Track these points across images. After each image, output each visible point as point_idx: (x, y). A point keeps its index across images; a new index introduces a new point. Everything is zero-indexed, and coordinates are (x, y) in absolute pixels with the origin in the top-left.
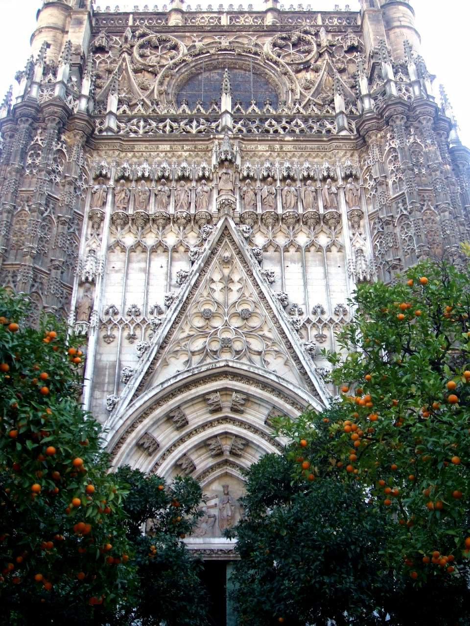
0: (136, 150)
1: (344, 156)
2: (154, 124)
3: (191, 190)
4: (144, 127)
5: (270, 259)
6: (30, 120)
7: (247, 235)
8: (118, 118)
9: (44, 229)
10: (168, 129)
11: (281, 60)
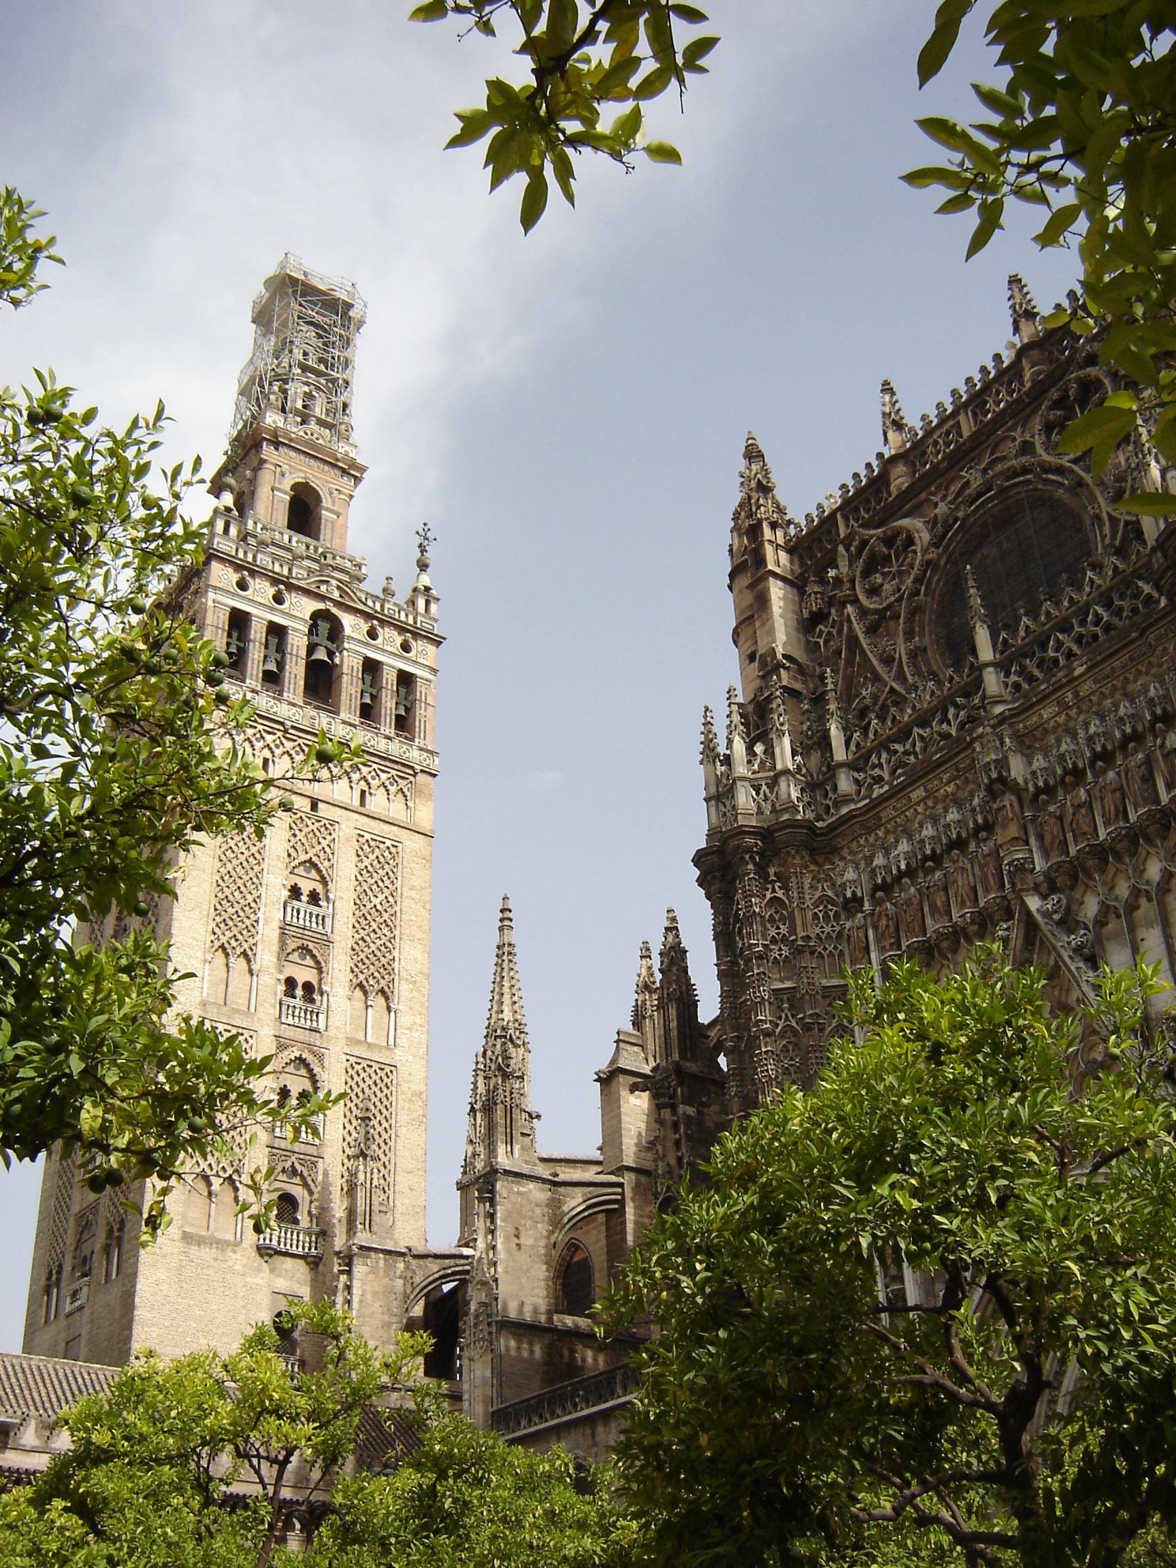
0: (884, 820)
2: (899, 747)
3: (971, 861)
4: (889, 761)
5: (1116, 936)
6: (718, 874)
7: (1056, 917)
8: (852, 766)
9: (788, 1051)
10: (919, 745)
11: (1064, 461)
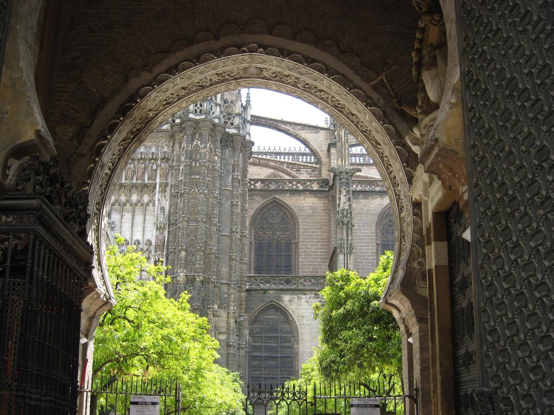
1: (165, 142)
5: (116, 210)
